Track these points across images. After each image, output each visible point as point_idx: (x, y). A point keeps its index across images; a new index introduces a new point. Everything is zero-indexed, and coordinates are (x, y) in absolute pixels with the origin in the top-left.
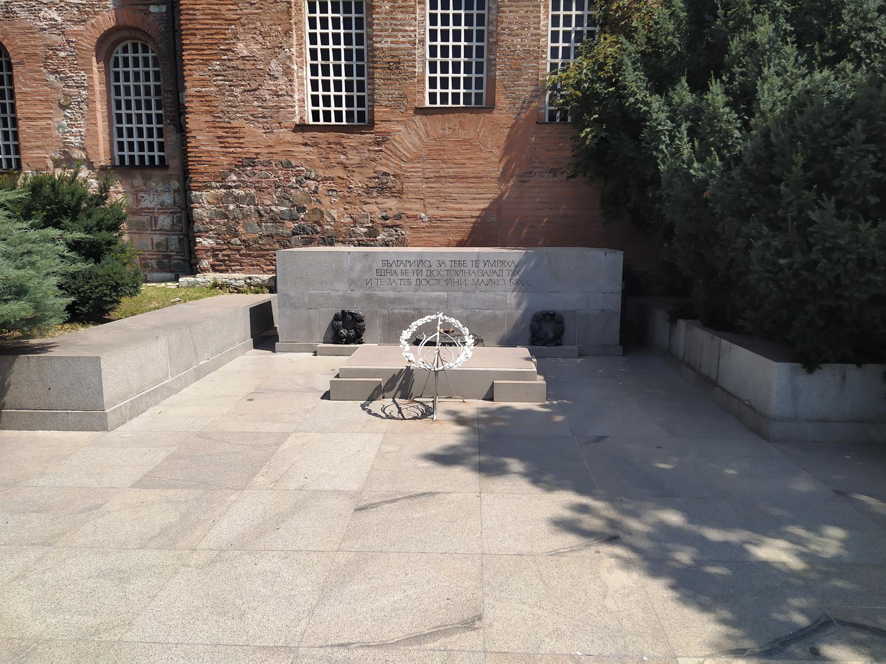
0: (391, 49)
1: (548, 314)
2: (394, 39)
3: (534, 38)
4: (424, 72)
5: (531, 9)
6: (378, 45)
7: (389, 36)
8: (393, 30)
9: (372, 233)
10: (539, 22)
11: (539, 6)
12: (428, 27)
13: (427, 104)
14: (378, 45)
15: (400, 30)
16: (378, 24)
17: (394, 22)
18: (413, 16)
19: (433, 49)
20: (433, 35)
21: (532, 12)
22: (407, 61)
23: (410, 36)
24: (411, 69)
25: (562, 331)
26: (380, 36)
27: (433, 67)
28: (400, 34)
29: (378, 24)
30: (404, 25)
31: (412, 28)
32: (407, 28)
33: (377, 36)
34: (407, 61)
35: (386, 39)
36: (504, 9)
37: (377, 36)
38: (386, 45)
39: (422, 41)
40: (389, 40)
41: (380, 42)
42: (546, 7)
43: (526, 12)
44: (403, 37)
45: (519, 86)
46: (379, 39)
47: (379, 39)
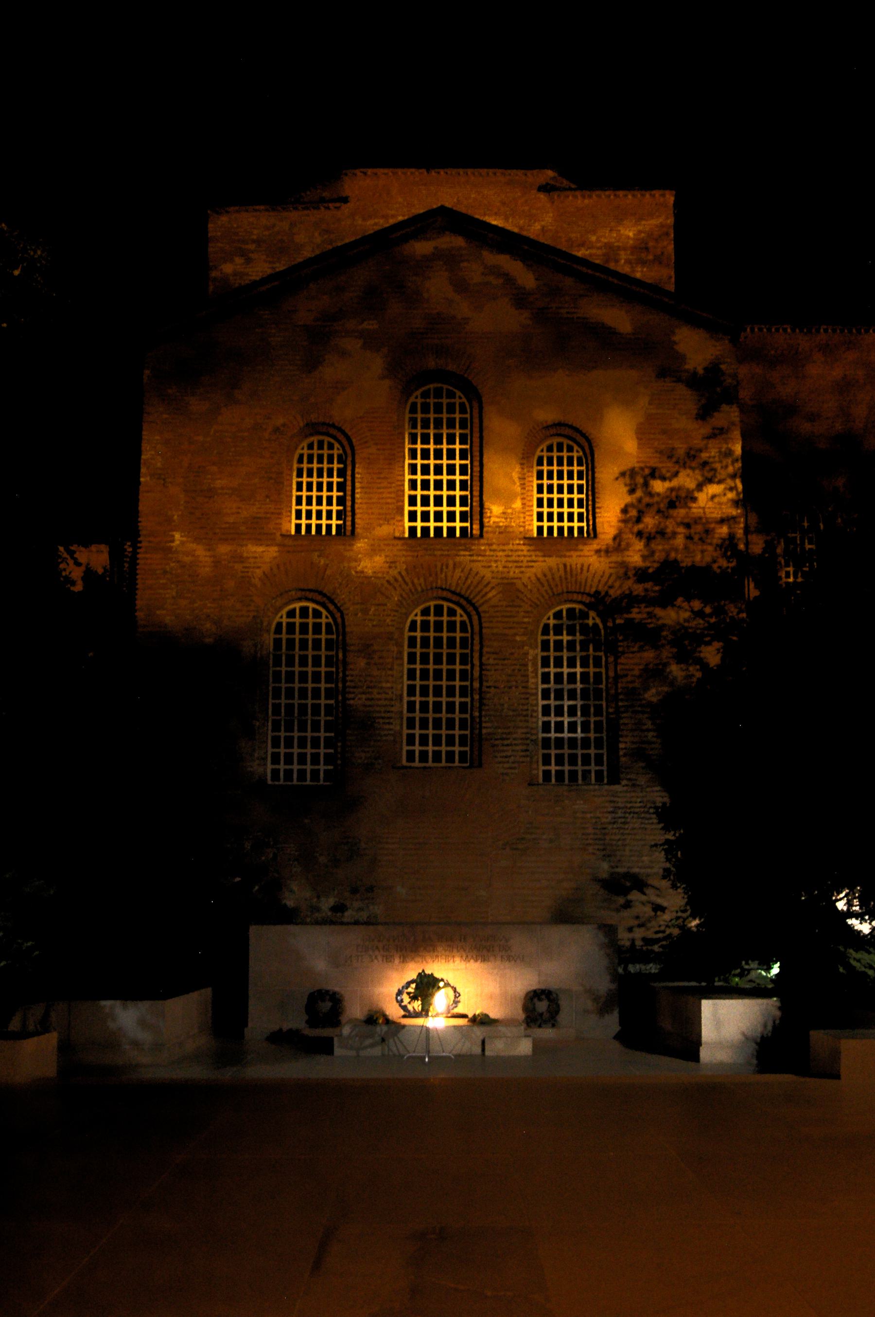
0: (365, 706)
1: (543, 992)
2: (368, 696)
3: (523, 696)
4: (402, 728)
5: (518, 667)
6: (352, 702)
7: (363, 693)
8: (368, 687)
9: (339, 908)
10: (527, 682)
11: (526, 665)
12: (406, 682)
13: (404, 762)
14: (352, 702)
15: (374, 687)
16: (351, 681)
17: (369, 679)
18: (390, 672)
19: (411, 706)
20: (411, 690)
21: (519, 670)
22: (383, 718)
23: (387, 693)
24: (387, 727)
25: (557, 1012)
26: (354, 693)
27: (411, 724)
28: (375, 691)
29: (351, 681)
30: (380, 682)
31: (389, 685)
32: (384, 685)
33: (350, 693)
34: (383, 718)
35: (359, 696)
36: (488, 667)
37: (350, 693)
38: (360, 702)
39: (401, 697)
40: (364, 696)
41: (353, 699)
42: (535, 665)
43: (514, 670)
44: (379, 693)
45: (508, 745)
46: (352, 696)
47: (352, 696)
